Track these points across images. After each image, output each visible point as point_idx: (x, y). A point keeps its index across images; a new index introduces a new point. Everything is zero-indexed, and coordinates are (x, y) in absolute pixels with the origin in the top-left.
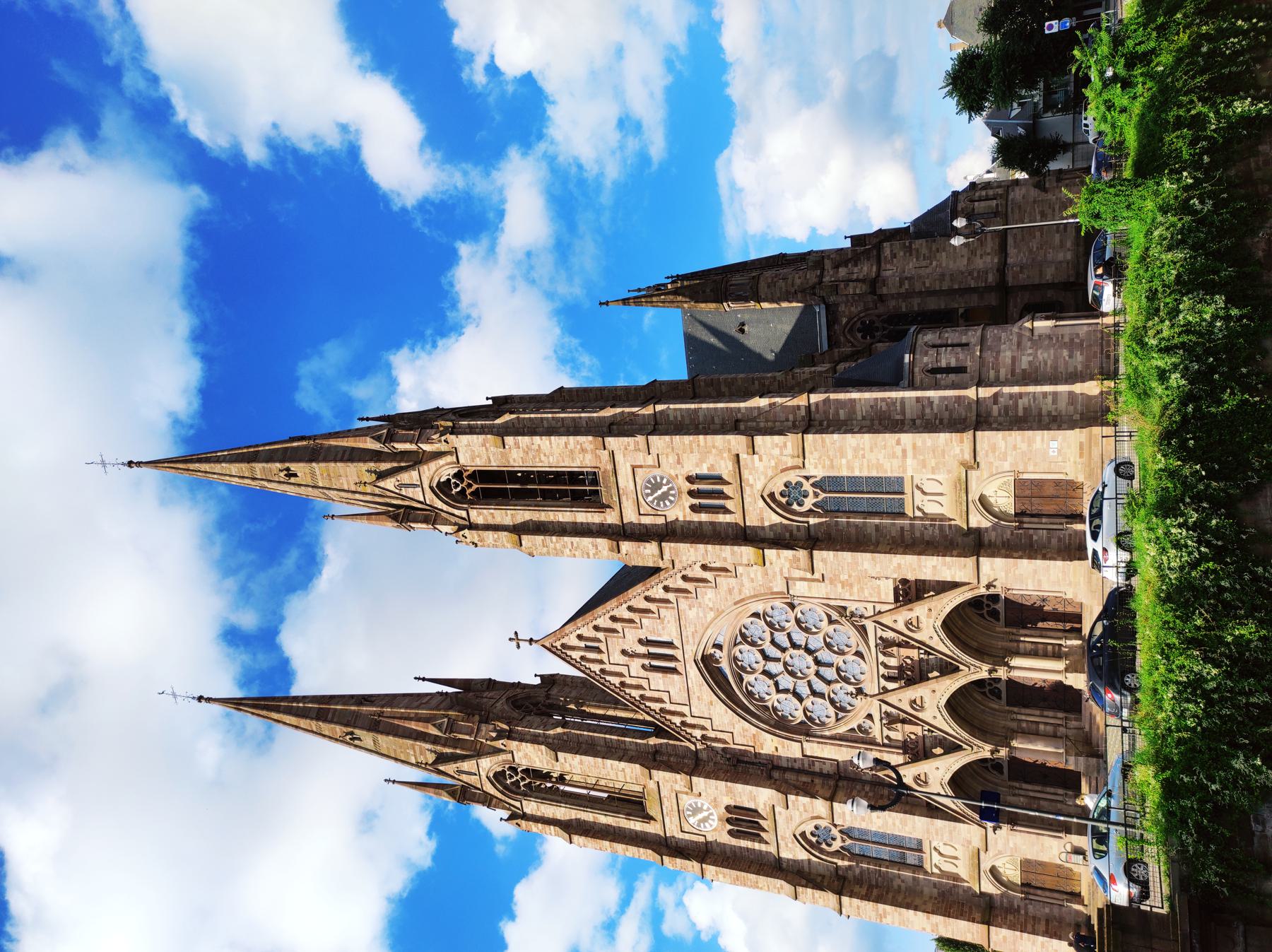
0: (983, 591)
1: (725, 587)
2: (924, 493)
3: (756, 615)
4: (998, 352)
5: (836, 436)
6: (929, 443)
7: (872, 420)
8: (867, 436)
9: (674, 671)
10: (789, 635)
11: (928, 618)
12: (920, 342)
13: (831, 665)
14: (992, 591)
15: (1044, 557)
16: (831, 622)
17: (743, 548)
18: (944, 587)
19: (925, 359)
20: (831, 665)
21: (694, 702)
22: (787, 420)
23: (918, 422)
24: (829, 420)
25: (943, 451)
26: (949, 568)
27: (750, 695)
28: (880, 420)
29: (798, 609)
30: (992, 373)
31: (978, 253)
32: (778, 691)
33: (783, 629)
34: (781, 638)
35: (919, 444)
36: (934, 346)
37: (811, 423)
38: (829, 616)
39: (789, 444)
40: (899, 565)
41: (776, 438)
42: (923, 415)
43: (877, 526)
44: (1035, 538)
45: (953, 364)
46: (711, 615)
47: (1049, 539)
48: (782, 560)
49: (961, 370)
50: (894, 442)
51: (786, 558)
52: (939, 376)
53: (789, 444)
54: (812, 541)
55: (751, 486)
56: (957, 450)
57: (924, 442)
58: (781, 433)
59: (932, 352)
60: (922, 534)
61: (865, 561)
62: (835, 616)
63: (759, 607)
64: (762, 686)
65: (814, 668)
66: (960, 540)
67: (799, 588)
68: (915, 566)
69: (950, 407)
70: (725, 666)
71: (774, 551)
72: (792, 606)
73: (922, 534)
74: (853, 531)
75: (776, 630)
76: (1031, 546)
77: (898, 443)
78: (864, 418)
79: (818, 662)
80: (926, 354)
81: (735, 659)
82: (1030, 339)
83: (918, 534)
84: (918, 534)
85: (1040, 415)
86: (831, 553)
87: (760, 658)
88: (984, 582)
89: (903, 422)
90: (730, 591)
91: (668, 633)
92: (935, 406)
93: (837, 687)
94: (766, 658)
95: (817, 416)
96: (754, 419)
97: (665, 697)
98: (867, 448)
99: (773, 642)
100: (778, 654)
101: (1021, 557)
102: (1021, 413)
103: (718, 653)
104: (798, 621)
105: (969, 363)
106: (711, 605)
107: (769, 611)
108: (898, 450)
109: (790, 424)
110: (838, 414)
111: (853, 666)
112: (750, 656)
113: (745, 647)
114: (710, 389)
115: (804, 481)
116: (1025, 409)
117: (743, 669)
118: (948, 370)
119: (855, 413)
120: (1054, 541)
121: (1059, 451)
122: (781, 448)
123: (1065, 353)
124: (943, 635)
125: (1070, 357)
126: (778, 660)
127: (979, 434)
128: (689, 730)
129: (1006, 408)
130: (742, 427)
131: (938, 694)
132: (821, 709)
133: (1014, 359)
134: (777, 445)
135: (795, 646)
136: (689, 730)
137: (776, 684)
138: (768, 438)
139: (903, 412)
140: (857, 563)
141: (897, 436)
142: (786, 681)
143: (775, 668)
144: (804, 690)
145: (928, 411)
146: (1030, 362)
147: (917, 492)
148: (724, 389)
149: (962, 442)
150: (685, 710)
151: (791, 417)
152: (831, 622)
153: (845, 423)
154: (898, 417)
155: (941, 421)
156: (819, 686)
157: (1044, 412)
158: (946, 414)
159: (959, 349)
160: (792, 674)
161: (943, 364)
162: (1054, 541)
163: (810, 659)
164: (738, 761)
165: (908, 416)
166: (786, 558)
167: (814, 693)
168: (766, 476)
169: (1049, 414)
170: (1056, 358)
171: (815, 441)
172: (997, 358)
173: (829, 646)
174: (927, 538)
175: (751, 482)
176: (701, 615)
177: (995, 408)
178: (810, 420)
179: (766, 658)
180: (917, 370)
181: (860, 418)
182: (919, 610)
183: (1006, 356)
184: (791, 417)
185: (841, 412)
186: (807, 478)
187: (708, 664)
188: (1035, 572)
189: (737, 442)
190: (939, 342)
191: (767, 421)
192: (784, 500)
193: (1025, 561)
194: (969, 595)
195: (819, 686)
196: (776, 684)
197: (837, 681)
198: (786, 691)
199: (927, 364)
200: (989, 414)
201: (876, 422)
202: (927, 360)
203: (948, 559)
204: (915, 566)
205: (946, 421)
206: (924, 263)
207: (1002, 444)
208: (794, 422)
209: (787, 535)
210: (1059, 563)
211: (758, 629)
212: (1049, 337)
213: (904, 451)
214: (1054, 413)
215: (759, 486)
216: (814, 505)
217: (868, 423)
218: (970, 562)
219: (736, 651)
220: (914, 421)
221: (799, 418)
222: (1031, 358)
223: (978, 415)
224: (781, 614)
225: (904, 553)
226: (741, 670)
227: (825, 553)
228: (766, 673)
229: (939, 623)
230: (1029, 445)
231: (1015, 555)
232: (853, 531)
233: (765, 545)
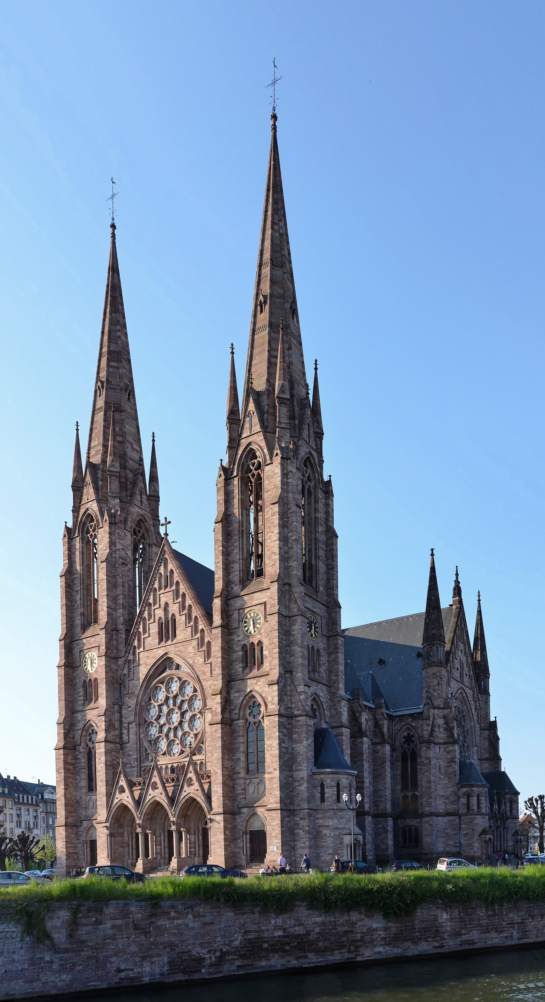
0: (208, 817)
1: (206, 670)
2: (258, 784)
3: (195, 690)
4: (332, 818)
5: (277, 734)
6: (275, 786)
7: (292, 753)
8: (277, 752)
9: (161, 640)
10: (187, 711)
11: (192, 790)
12: (341, 776)
13: (175, 736)
14: (209, 821)
15: (226, 846)
16: (196, 735)
17: (220, 681)
18: (208, 797)
19: (329, 780)
20: (175, 736)
21: (146, 654)
22: (292, 703)
23: (291, 779)
24: (291, 729)
25: (271, 794)
26: (217, 799)
27: (156, 688)
28: (292, 758)
29: (199, 715)
30: (320, 816)
31: (447, 801)
32: (160, 706)
33: (190, 706)
34: (185, 706)
35: (274, 781)
36: (338, 785)
37: (286, 718)
38: (199, 733)
39: (273, 707)
40: (217, 773)
41: (276, 699)
42: (295, 781)
43: (239, 759)
44: (239, 841)
45: (326, 795)
46: (191, 662)
47: (239, 848)
48: (215, 706)
49: (323, 799)
50: (275, 767)
51: (216, 708)
52: (319, 788)
53: (273, 707)
54: (227, 723)
55: (257, 684)
56: (272, 801)
57: (275, 783)
58: (280, 701)
59: (333, 783)
60: (237, 784)
61: (218, 754)
62: (199, 736)
63: (199, 693)
64: (161, 696)
65: (172, 726)
66: (236, 804)
67: (209, 716)
68: (217, 781)
69: (299, 796)
70: (168, 672)
71: (219, 701)
72: (200, 712)
73: (237, 784)
74: (237, 746)
75: (189, 703)
76: (235, 839)
77: (275, 769)
78: (293, 749)
79: (176, 728)
80: (332, 781)
81: (173, 678)
82: (340, 834)
83: (237, 782)
84: (237, 782)
85: (294, 841)
86: (220, 735)
87: (175, 693)
88: (213, 817)
89: (292, 770)
90: (204, 673)
91: (183, 632)
92: (299, 787)
93: (165, 740)
94: (175, 697)
95: (294, 721)
96: (292, 682)
97: (147, 635)
98: (272, 752)
99: (183, 701)
100: (178, 704)
101: (225, 834)
102: (296, 831)
103: (174, 667)
104: (194, 716)
105: (326, 803)
106: (196, 661)
107: (198, 698)
108: (271, 770)
109: (289, 706)
110: (295, 733)
111: (176, 749)
112: (175, 687)
113: (178, 684)
114: (332, 647)
115: (261, 716)
116: (298, 833)
117: (168, 683)
118: (323, 793)
119: (296, 743)
120: (238, 850)
121: (272, 851)
122: (271, 702)
123: (331, 851)
124: (187, 798)
125: (329, 854)
126: (174, 705)
127: (279, 812)
128: (131, 651)
129: (298, 824)
130: (287, 675)
131: (160, 796)
132: (154, 731)
133: (328, 826)
134: (273, 699)
135: (183, 714)
136: (131, 651)
137: (162, 705)
138: (276, 693)
139: (297, 770)
140: (216, 750)
141: (278, 769)
142: (165, 709)
143: (171, 702)
144: (162, 721)
145: (297, 784)
146: (326, 834)
147: (258, 780)
148: (333, 656)
149: (276, 803)
150: (142, 649)
151: (293, 706)
152: (196, 735)
153: (291, 738)
154: (294, 768)
155: (290, 791)
156: (165, 730)
157: (296, 843)
158: (295, 794)
159: (335, 797)
160: (169, 713)
161: (326, 790)
162: (238, 850)
163: (176, 724)
164: (121, 684)
165: (295, 774)
166: (216, 708)
167: (161, 727)
168: (263, 692)
169: (295, 845)
170: (327, 847)
171: (275, 722)
172: (328, 818)
173: (184, 734)
174: (236, 786)
175: (259, 683)
176: (190, 655)
177: (298, 819)
178: (292, 717)
179: (175, 697)
180: (323, 776)
181: (294, 746)
182: (196, 785)
183: (330, 823)
184: (293, 706)
185: (296, 735)
186: (263, 718)
187: (165, 663)
188: (219, 842)
189: (275, 675)
190: (341, 787)
191: (291, 691)
192: (251, 704)
193: (223, 837)
194: (206, 810)
195: (165, 730)
196: (162, 705)
197: (168, 740)
198: (160, 711)
199: (326, 781)
200: (294, 815)
201: (290, 756)
202: (329, 780)
203: (222, 798)
204: (217, 781)
205: (291, 794)
206: (443, 771)
207: (275, 823)
208: (291, 708)
209: (233, 707)
210: (223, 853)
211: (189, 691)
212: (341, 843)
213: (271, 773)
214: (296, 847)
215: (257, 688)
216: (250, 722)
217: (290, 751)
218: (221, 810)
219: (176, 679)
220: (292, 776)
221: (293, 711)
222: (328, 835)
223: (294, 810)
224: (198, 704)
225: (223, 775)
226: (168, 682)
227: (220, 731)
228: (167, 698)
229: (192, 795)
230: (275, 837)
231: (228, 832)
232: (237, 746)
233: (224, 694)
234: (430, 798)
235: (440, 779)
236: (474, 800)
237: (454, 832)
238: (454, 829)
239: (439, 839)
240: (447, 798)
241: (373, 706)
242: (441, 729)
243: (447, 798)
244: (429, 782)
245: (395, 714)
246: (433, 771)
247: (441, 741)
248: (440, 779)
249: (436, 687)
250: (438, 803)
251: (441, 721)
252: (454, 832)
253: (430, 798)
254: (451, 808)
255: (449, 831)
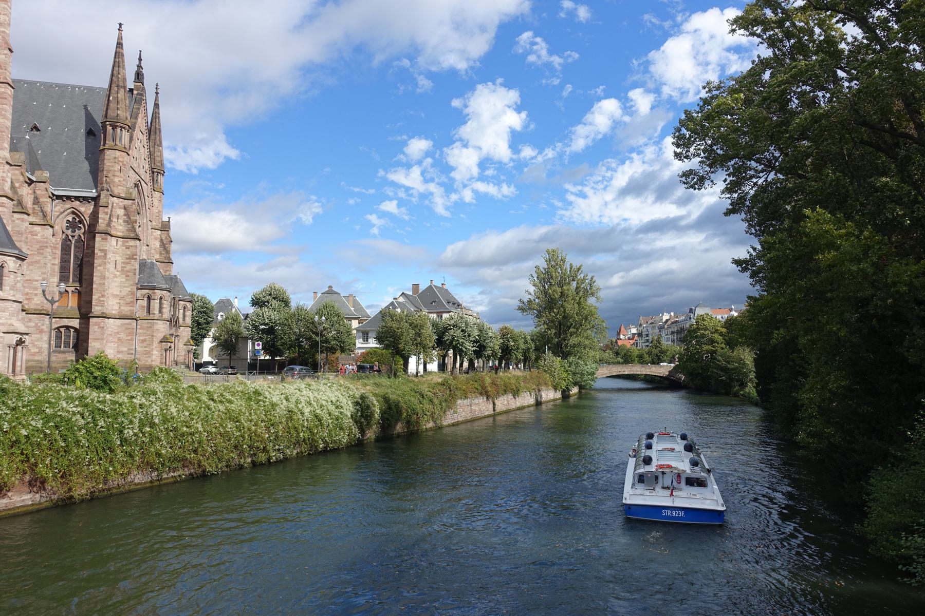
234: (103, 296)
235: (115, 276)
236: (155, 304)
237: (129, 338)
238: (130, 334)
239: (109, 344)
240: (122, 298)
241: (34, 179)
242: (121, 221)
243: (122, 298)
244: (103, 277)
245: (56, 193)
246: (108, 266)
247: (120, 234)
248: (115, 276)
249: (118, 174)
250: (110, 303)
251: (121, 212)
252: (129, 338)
253: (103, 296)
254: (126, 310)
255: (122, 335)
